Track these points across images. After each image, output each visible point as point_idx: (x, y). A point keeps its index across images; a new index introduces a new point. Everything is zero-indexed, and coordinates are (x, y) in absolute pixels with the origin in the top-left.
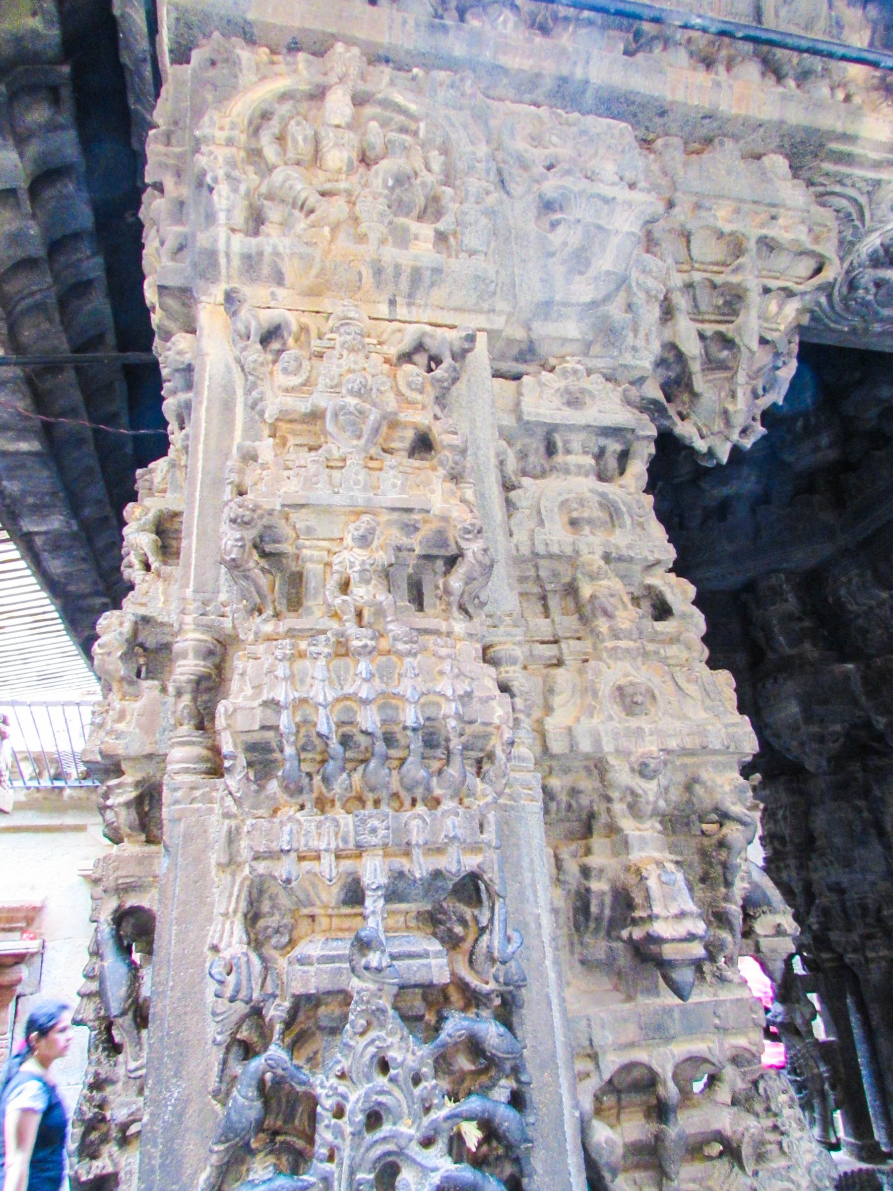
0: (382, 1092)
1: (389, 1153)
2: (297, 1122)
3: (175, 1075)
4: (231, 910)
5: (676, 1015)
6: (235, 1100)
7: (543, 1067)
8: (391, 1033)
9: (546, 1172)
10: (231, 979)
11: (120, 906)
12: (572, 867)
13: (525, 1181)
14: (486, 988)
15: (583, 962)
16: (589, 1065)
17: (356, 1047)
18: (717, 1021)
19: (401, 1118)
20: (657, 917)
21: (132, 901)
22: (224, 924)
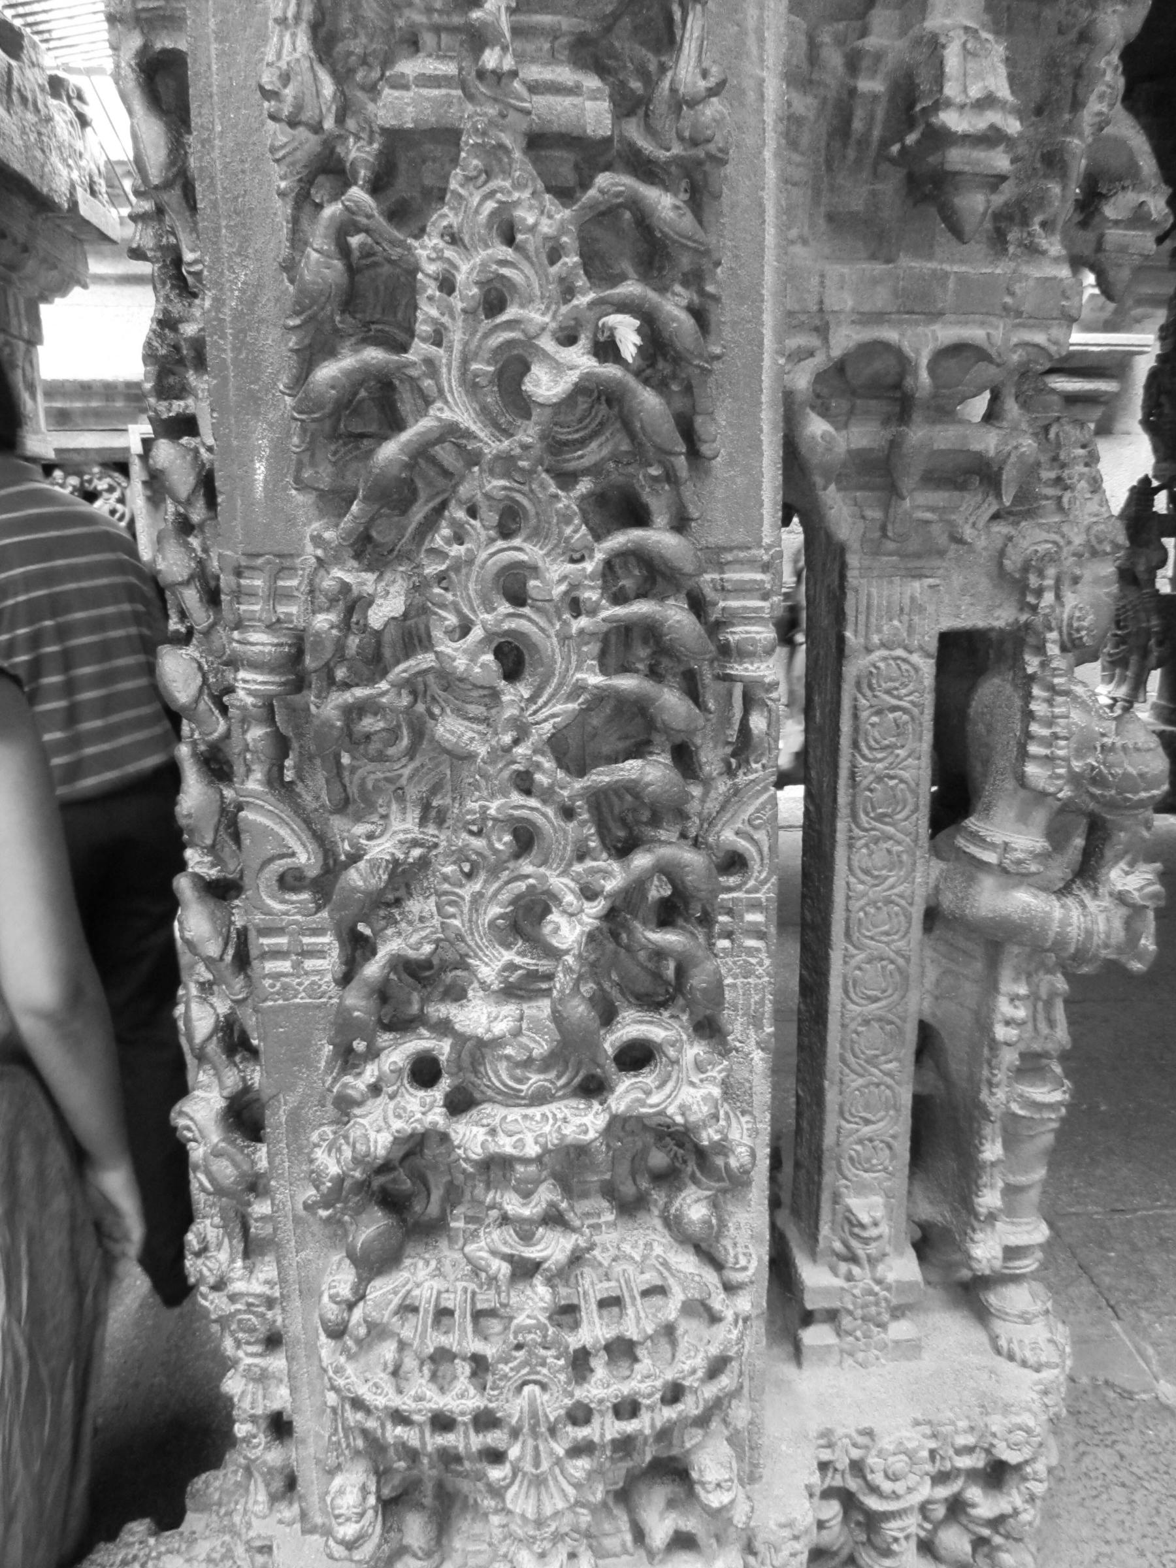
0: (503, 263)
1: (510, 343)
2: (400, 315)
3: (239, 254)
4: (290, 14)
5: (951, 284)
6: (308, 257)
7: (741, 298)
8: (518, 186)
9: (730, 424)
10: (289, 92)
11: (145, 48)
12: (834, 59)
13: (699, 420)
14: (663, 155)
15: (831, 218)
16: (814, 341)
17: (469, 203)
18: (1008, 300)
19: (531, 301)
20: (948, 104)
21: (164, 42)
22: (281, 37)
